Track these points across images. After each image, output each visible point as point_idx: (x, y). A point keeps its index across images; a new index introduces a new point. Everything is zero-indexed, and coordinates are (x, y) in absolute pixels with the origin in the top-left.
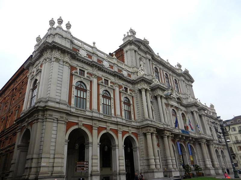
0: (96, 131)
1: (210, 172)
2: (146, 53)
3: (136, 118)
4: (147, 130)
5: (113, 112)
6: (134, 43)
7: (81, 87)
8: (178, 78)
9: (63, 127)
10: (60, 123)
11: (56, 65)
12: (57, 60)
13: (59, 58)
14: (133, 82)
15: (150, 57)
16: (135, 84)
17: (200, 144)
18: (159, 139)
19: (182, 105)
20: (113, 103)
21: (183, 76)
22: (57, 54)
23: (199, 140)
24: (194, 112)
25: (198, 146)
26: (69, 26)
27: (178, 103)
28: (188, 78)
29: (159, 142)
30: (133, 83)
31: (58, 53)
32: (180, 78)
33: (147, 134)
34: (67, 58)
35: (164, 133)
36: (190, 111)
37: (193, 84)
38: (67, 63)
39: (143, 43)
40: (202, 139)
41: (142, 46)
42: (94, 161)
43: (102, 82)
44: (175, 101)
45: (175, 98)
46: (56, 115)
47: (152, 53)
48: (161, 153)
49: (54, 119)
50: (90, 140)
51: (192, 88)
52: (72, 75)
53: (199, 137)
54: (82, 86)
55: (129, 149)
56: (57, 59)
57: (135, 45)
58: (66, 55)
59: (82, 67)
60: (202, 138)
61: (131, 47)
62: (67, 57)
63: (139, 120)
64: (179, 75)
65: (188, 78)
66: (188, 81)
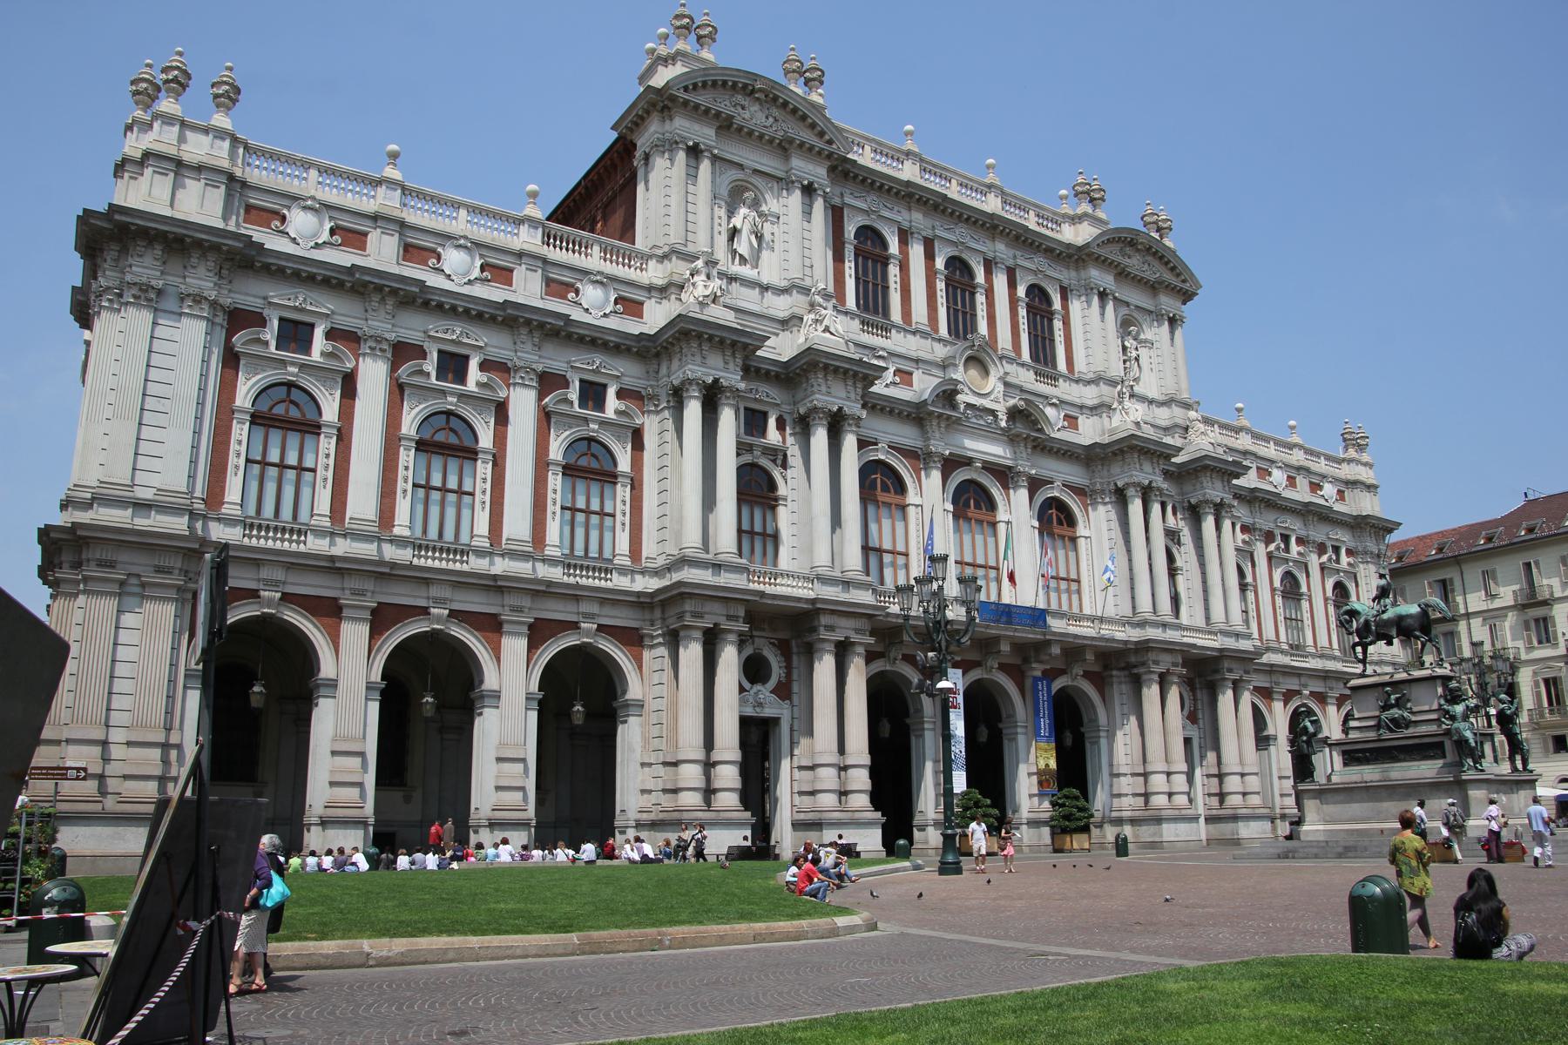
0: (364, 629)
2: (784, 148)
3: (649, 548)
4: (681, 617)
5: (482, 527)
6: (686, 103)
7: (287, 411)
8: (1066, 275)
9: (164, 614)
10: (155, 598)
11: (138, 319)
12: (150, 297)
13: (153, 283)
14: (648, 349)
15: (817, 172)
16: (657, 355)
17: (1137, 684)
18: (795, 658)
19: (1044, 447)
20: (484, 480)
21: (1104, 263)
22: (145, 267)
23: (1133, 659)
24: (1131, 492)
25: (1119, 691)
27: (1012, 439)
28: (1154, 272)
29: (789, 674)
30: (650, 350)
31: (148, 260)
32: (1083, 274)
33: (682, 634)
34: (201, 279)
35: (814, 630)
36: (1112, 487)
37: (1188, 310)
38: (198, 299)
39: (760, 90)
40: (1149, 649)
41: (756, 107)
43: (421, 372)
44: (989, 433)
45: (993, 412)
48: (792, 730)
49: (122, 583)
50: (327, 669)
53: (1126, 642)
54: (297, 405)
55: (578, 708)
56: (144, 288)
58: (194, 261)
59: (295, 308)
60: (1144, 647)
61: (668, 126)
62: (202, 271)
63: (661, 561)
64: (1070, 256)
66: (1153, 288)
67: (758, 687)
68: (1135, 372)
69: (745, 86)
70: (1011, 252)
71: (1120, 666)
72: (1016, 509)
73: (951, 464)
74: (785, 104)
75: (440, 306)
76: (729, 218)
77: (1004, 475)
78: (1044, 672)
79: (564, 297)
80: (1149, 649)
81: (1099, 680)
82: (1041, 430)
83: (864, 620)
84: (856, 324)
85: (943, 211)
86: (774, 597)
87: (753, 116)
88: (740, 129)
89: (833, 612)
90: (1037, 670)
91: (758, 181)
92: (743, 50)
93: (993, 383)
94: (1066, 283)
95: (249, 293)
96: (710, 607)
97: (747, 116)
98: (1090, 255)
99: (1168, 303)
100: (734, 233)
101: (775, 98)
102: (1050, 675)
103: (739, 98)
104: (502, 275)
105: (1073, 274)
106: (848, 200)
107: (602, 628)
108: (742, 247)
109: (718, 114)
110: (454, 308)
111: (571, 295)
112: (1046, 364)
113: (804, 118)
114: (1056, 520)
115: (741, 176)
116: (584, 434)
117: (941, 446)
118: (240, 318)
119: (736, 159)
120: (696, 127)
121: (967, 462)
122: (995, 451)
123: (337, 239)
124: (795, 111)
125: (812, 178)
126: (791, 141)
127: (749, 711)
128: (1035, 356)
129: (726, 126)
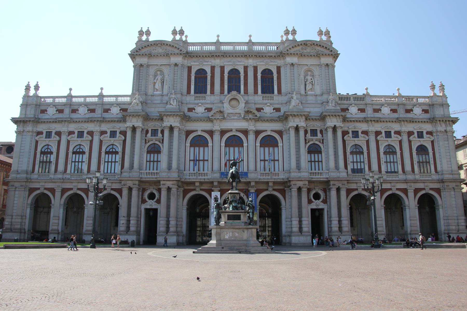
1: (291, 240)
2: (167, 55)
6: (137, 55)
8: (279, 62)
15: (179, 60)
19: (259, 120)
26: (37, 88)
27: (247, 120)
39: (159, 44)
42: (56, 221)
46: (16, 184)
47: (181, 50)
51: (330, 67)
52: (37, 142)
57: (146, 53)
65: (323, 51)
67: (151, 201)
68: (309, 87)
69: (154, 44)
70: (255, 61)
71: (284, 186)
72: (251, 142)
73: (223, 132)
74: (167, 44)
75: (76, 121)
76: (154, 79)
77: (245, 132)
78: (256, 191)
79: (107, 112)
80: (290, 181)
81: (283, 192)
82: (256, 116)
83: (175, 182)
84: (193, 98)
85: (226, 56)
86: (145, 178)
87: (160, 50)
88: (154, 56)
89: (164, 180)
90: (252, 190)
91: (163, 68)
92: (161, 33)
93: (242, 105)
94: (279, 65)
95: (43, 128)
96: (128, 182)
97: (156, 51)
98: (285, 54)
99: (324, 60)
100: (155, 83)
101: (164, 44)
102: (258, 192)
103: (154, 48)
104: (93, 111)
105: (282, 61)
106: (192, 64)
107: (112, 189)
108: (157, 86)
109: (146, 54)
110: (79, 121)
111: (109, 111)
112: (270, 93)
113: (173, 46)
114: (269, 142)
115: (157, 68)
116: (111, 144)
117: (217, 126)
118: (39, 133)
119: (155, 64)
120: (142, 59)
121: (231, 130)
122: (243, 125)
123: (58, 112)
124: (170, 45)
125: (176, 62)
126: (168, 54)
127: (148, 207)
128: (263, 92)
129: (150, 56)
